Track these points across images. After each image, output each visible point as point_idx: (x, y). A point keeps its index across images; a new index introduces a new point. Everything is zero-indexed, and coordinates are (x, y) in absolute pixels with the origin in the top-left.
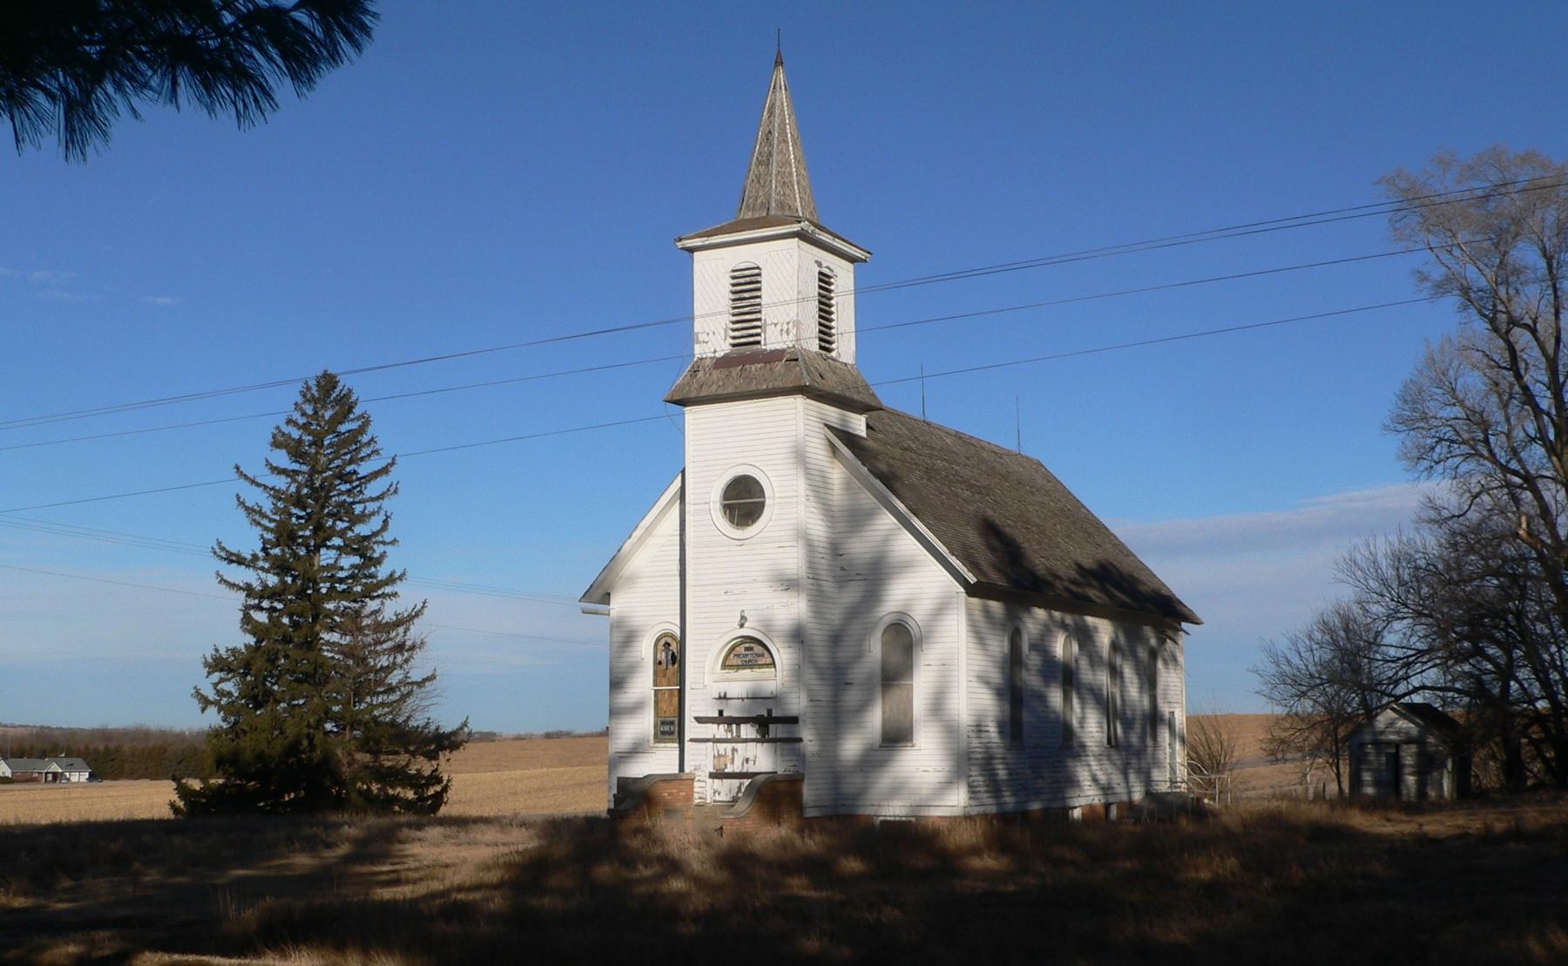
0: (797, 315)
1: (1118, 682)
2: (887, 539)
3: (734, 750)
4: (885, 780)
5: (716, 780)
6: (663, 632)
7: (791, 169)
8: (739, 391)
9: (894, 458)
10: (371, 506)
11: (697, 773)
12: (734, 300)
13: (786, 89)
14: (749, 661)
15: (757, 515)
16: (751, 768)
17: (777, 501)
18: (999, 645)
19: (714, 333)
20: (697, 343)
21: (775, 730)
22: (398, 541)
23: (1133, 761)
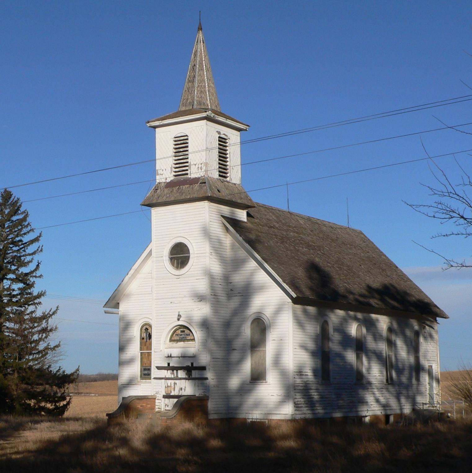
0: (206, 160)
1: (393, 348)
2: (252, 274)
3: (175, 384)
4: (251, 400)
5: (166, 399)
6: (144, 323)
7: (205, 84)
8: (176, 199)
9: (261, 232)
10: (28, 258)
11: (157, 395)
12: (175, 152)
13: (203, 43)
14: (183, 338)
15: (186, 263)
16: (183, 393)
17: (196, 255)
18: (312, 328)
19: (166, 170)
20: (158, 175)
21: (195, 374)
22: (43, 276)
23: (403, 392)
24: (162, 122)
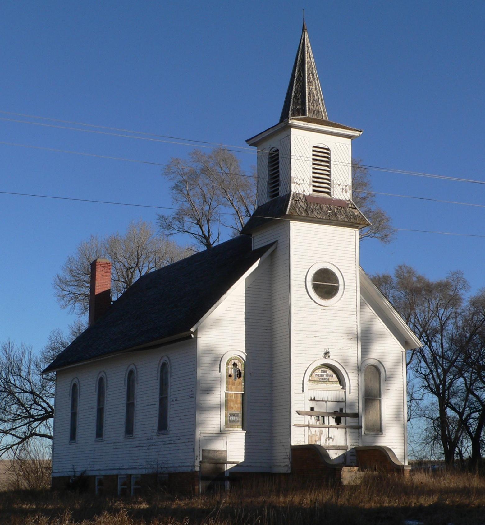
3: (321, 433)
15: (334, 293)
19: (303, 180)
24: (307, 124)
